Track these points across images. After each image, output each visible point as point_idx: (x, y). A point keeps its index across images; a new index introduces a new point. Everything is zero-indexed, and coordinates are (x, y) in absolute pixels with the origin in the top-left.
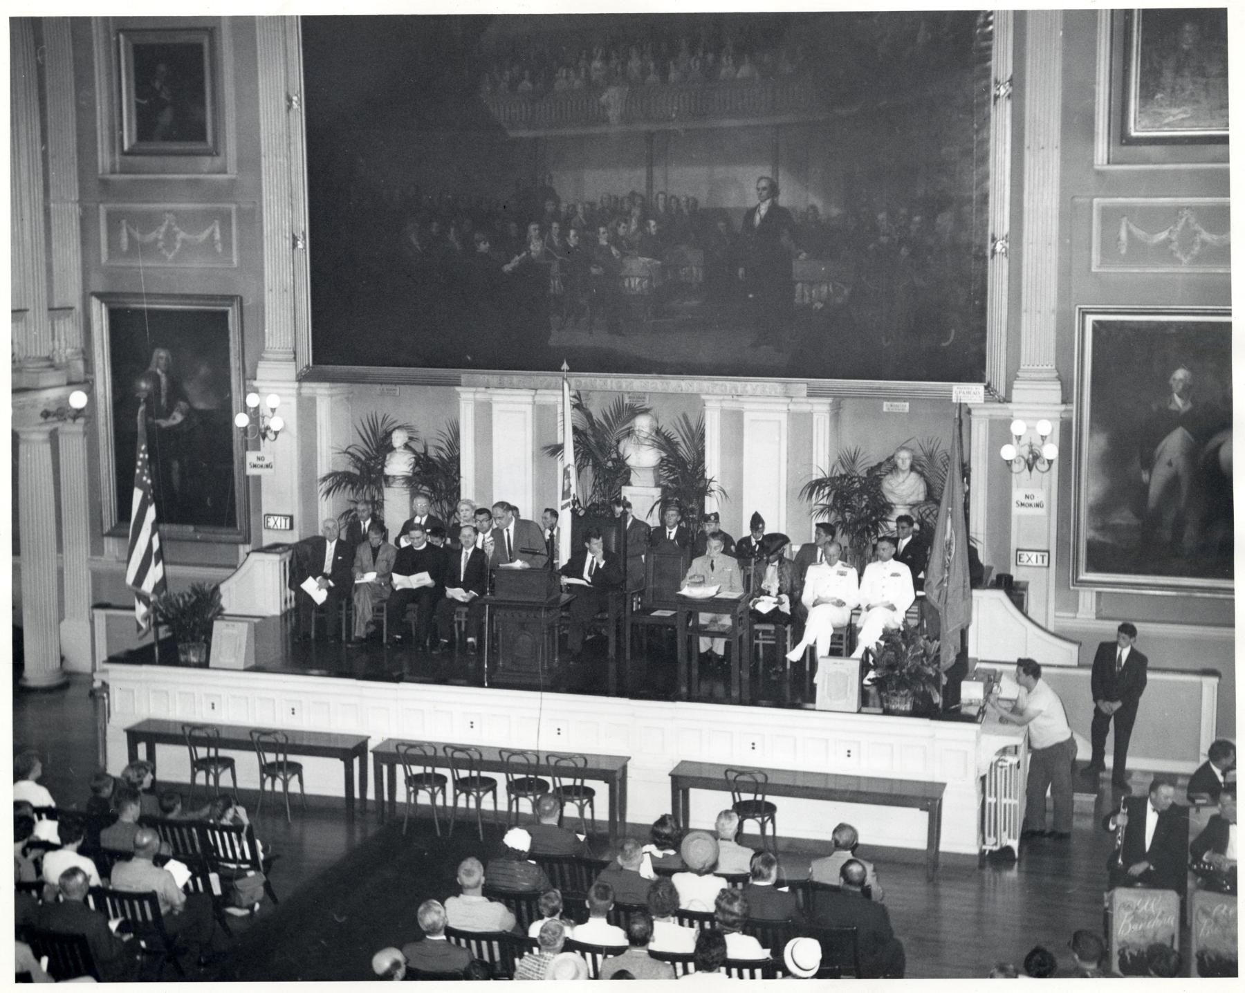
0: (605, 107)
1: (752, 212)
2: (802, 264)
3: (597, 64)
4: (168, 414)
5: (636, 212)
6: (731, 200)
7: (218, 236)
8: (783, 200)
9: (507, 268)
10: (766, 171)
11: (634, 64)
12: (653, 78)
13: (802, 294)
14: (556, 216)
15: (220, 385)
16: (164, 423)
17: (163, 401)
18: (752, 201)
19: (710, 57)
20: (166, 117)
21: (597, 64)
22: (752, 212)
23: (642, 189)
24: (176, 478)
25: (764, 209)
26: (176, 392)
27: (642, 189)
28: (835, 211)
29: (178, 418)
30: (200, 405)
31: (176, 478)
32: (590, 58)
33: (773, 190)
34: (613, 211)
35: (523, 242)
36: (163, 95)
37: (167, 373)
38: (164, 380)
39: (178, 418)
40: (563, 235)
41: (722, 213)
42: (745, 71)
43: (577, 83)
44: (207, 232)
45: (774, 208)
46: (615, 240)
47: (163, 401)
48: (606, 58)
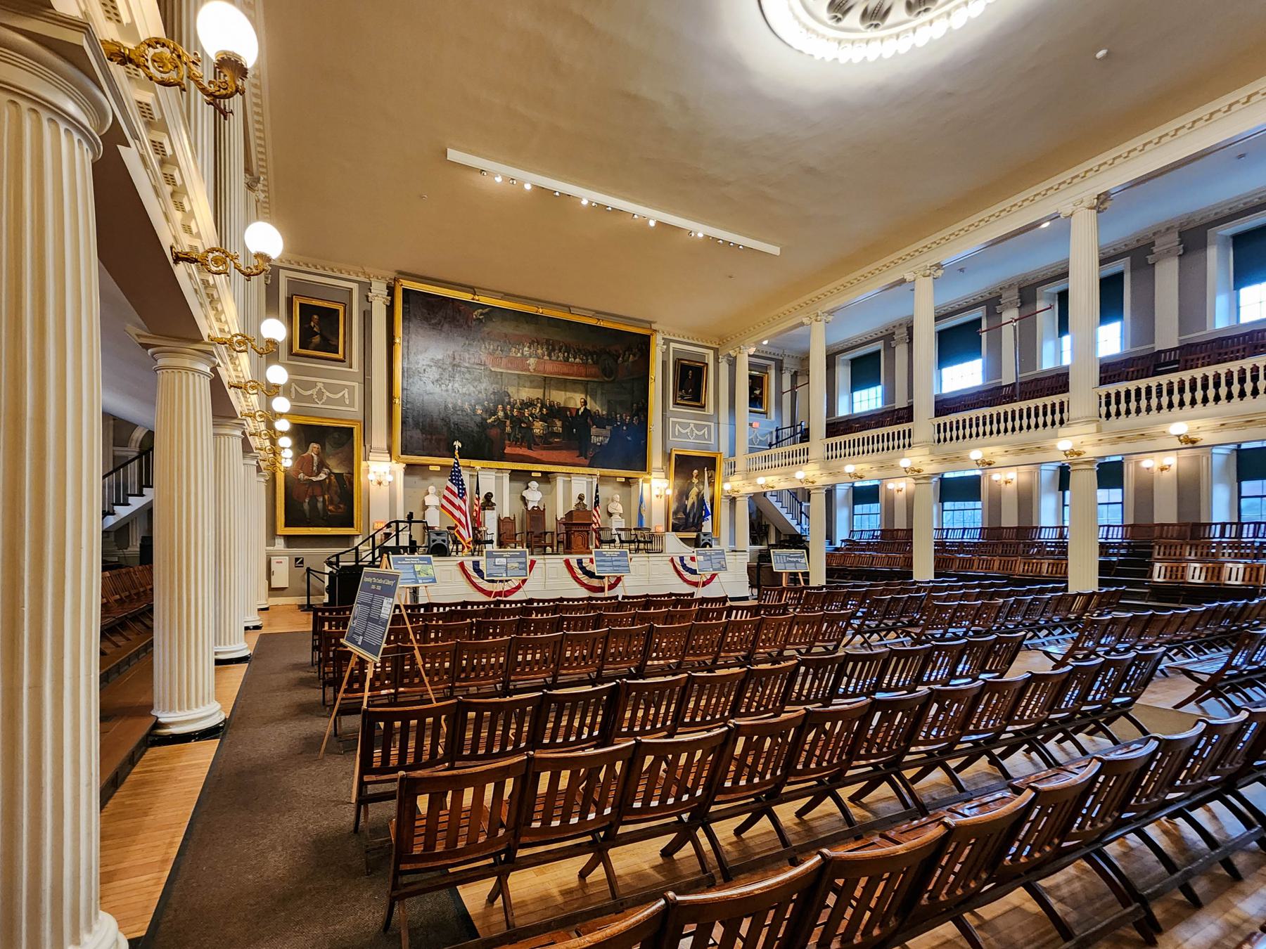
0: (529, 365)
1: (578, 410)
2: (594, 430)
3: (526, 349)
4: (317, 475)
5: (539, 405)
6: (571, 405)
7: (346, 396)
8: (588, 407)
9: (489, 421)
10: (583, 396)
11: (540, 351)
12: (546, 358)
13: (594, 439)
14: (509, 403)
15: (349, 461)
16: (314, 479)
17: (315, 468)
18: (578, 407)
19: (566, 354)
20: (317, 339)
21: (526, 349)
22: (578, 410)
23: (541, 397)
24: (320, 505)
25: (582, 409)
26: (322, 465)
27: (541, 397)
28: (604, 413)
29: (323, 476)
30: (336, 471)
31: (320, 505)
32: (524, 346)
33: (585, 403)
34: (530, 404)
35: (494, 413)
36: (315, 329)
37: (318, 455)
38: (316, 458)
39: (323, 476)
40: (512, 411)
41: (569, 409)
42: (577, 360)
43: (519, 355)
44: (341, 394)
45: (585, 409)
46: (531, 415)
47: (315, 468)
48: (530, 347)
